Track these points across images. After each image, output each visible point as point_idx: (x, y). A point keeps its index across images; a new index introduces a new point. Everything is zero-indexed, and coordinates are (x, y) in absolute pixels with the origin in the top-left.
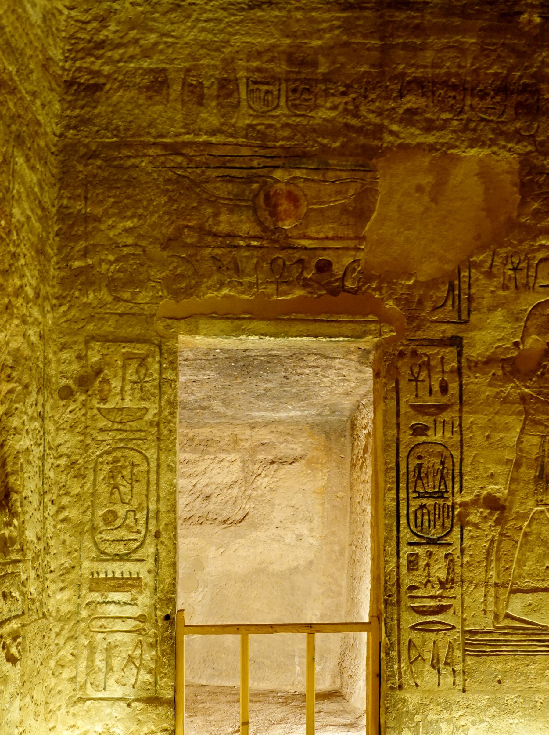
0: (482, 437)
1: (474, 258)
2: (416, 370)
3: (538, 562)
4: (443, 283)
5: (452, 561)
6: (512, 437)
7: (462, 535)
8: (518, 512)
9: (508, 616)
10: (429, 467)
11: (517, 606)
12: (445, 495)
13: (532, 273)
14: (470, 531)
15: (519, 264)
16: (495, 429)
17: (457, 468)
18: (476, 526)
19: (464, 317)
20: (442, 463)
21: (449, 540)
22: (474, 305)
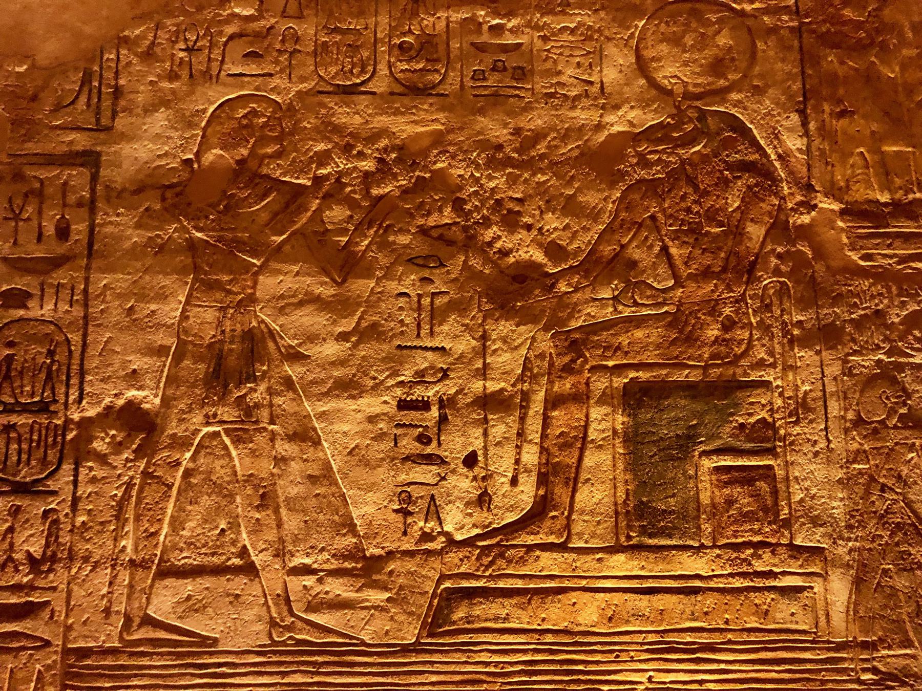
0: (120, 310)
1: (126, 33)
2: (18, 201)
3: (206, 521)
4: (76, 69)
5: (56, 522)
6: (171, 311)
7: (76, 475)
8: (175, 434)
9: (148, 621)
10: (26, 361)
11: (164, 602)
12: (52, 408)
13: (216, 54)
14: (91, 469)
15: (195, 42)
16: (143, 297)
17: (76, 361)
18: (102, 459)
19: (104, 122)
20: (51, 353)
21: (52, 485)
22: (122, 103)
